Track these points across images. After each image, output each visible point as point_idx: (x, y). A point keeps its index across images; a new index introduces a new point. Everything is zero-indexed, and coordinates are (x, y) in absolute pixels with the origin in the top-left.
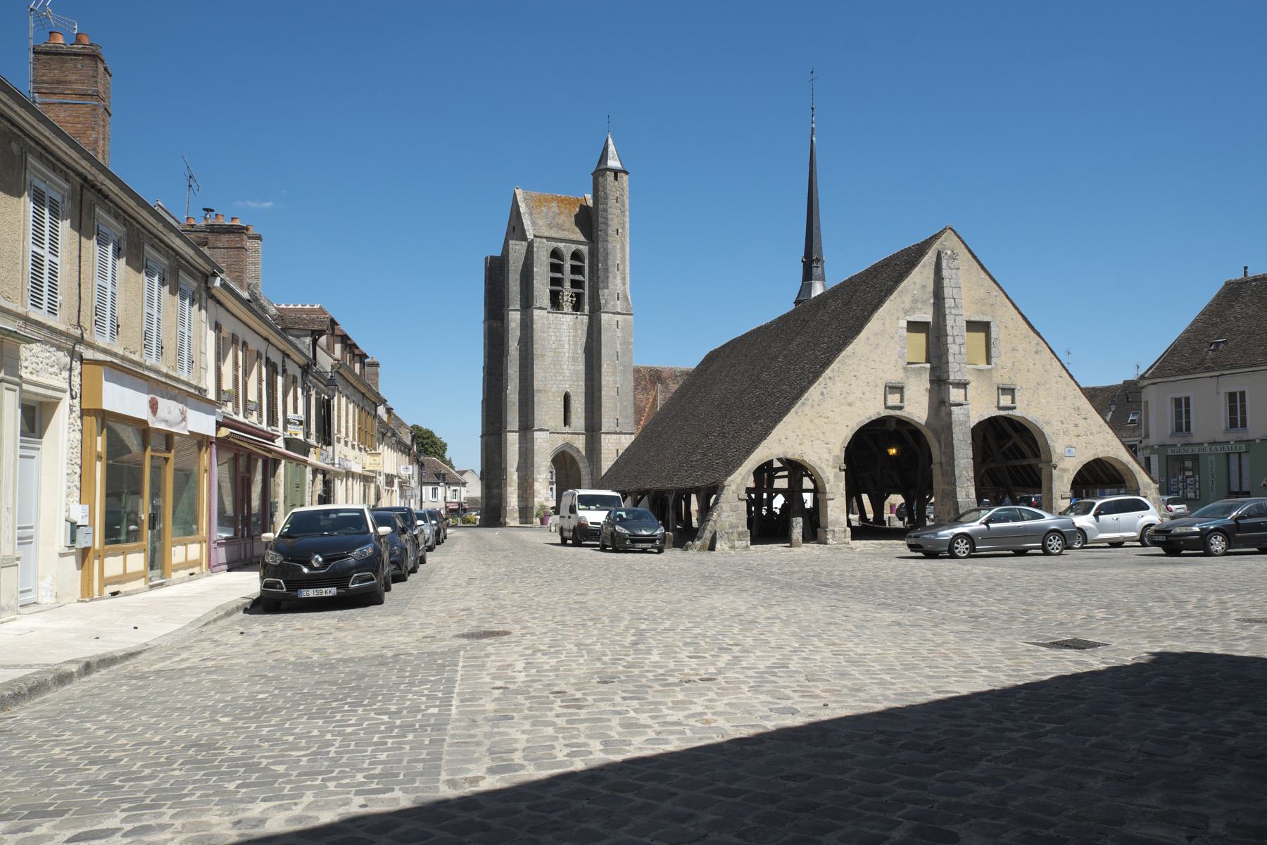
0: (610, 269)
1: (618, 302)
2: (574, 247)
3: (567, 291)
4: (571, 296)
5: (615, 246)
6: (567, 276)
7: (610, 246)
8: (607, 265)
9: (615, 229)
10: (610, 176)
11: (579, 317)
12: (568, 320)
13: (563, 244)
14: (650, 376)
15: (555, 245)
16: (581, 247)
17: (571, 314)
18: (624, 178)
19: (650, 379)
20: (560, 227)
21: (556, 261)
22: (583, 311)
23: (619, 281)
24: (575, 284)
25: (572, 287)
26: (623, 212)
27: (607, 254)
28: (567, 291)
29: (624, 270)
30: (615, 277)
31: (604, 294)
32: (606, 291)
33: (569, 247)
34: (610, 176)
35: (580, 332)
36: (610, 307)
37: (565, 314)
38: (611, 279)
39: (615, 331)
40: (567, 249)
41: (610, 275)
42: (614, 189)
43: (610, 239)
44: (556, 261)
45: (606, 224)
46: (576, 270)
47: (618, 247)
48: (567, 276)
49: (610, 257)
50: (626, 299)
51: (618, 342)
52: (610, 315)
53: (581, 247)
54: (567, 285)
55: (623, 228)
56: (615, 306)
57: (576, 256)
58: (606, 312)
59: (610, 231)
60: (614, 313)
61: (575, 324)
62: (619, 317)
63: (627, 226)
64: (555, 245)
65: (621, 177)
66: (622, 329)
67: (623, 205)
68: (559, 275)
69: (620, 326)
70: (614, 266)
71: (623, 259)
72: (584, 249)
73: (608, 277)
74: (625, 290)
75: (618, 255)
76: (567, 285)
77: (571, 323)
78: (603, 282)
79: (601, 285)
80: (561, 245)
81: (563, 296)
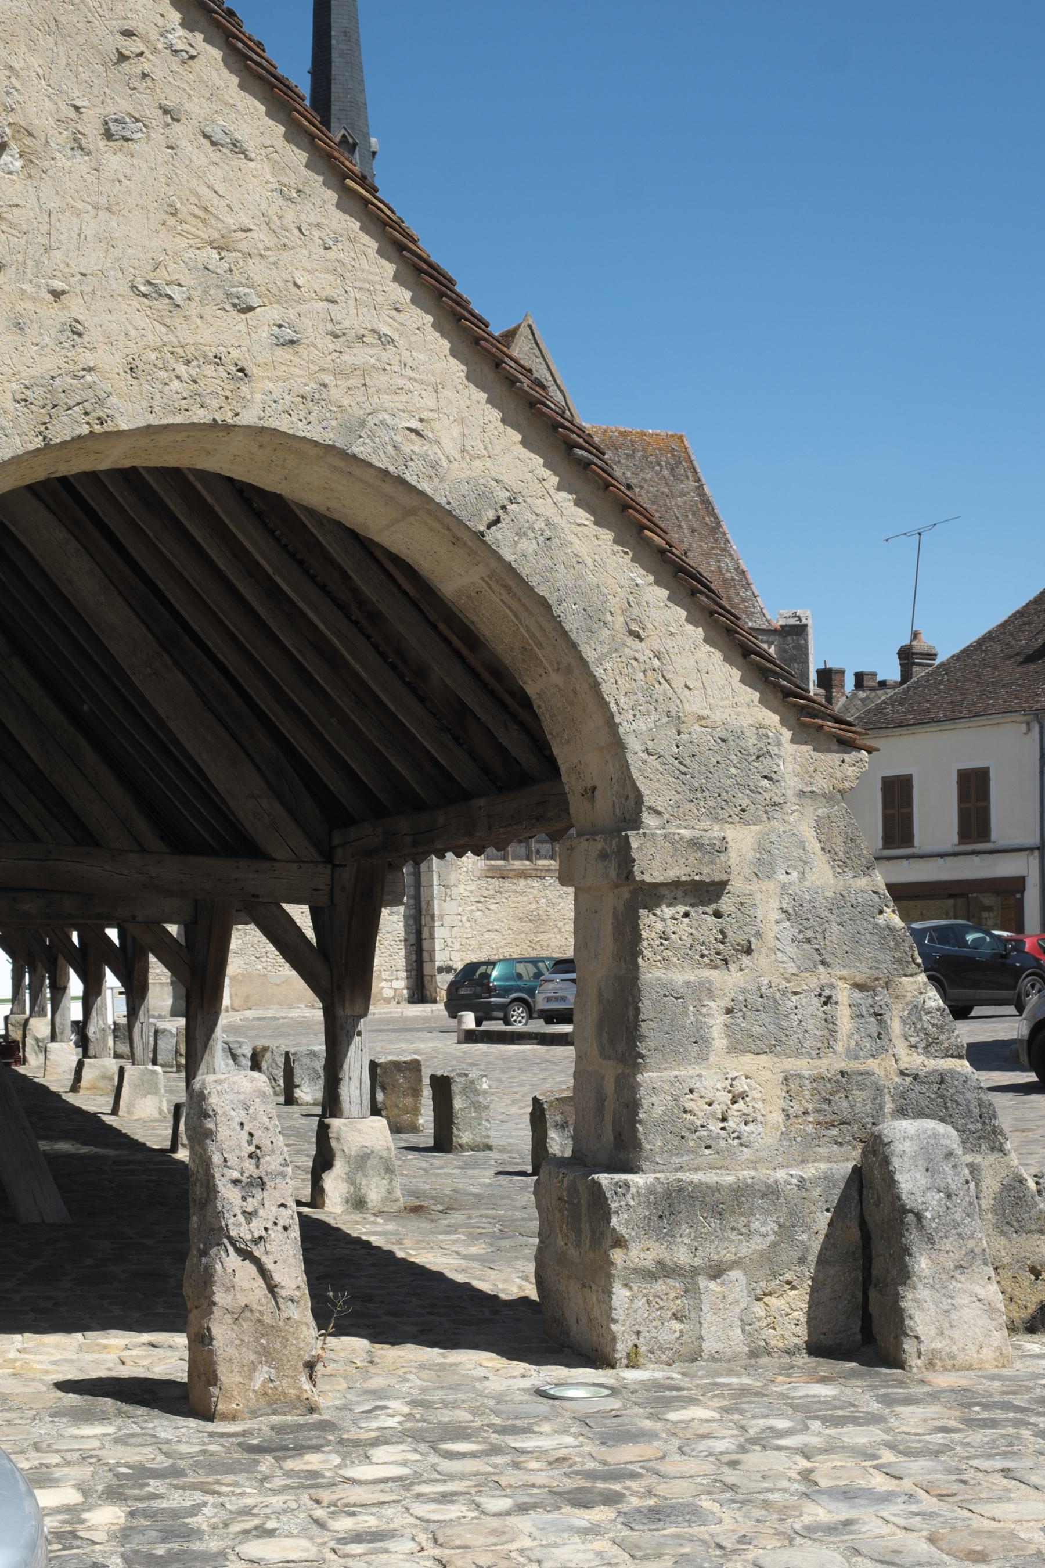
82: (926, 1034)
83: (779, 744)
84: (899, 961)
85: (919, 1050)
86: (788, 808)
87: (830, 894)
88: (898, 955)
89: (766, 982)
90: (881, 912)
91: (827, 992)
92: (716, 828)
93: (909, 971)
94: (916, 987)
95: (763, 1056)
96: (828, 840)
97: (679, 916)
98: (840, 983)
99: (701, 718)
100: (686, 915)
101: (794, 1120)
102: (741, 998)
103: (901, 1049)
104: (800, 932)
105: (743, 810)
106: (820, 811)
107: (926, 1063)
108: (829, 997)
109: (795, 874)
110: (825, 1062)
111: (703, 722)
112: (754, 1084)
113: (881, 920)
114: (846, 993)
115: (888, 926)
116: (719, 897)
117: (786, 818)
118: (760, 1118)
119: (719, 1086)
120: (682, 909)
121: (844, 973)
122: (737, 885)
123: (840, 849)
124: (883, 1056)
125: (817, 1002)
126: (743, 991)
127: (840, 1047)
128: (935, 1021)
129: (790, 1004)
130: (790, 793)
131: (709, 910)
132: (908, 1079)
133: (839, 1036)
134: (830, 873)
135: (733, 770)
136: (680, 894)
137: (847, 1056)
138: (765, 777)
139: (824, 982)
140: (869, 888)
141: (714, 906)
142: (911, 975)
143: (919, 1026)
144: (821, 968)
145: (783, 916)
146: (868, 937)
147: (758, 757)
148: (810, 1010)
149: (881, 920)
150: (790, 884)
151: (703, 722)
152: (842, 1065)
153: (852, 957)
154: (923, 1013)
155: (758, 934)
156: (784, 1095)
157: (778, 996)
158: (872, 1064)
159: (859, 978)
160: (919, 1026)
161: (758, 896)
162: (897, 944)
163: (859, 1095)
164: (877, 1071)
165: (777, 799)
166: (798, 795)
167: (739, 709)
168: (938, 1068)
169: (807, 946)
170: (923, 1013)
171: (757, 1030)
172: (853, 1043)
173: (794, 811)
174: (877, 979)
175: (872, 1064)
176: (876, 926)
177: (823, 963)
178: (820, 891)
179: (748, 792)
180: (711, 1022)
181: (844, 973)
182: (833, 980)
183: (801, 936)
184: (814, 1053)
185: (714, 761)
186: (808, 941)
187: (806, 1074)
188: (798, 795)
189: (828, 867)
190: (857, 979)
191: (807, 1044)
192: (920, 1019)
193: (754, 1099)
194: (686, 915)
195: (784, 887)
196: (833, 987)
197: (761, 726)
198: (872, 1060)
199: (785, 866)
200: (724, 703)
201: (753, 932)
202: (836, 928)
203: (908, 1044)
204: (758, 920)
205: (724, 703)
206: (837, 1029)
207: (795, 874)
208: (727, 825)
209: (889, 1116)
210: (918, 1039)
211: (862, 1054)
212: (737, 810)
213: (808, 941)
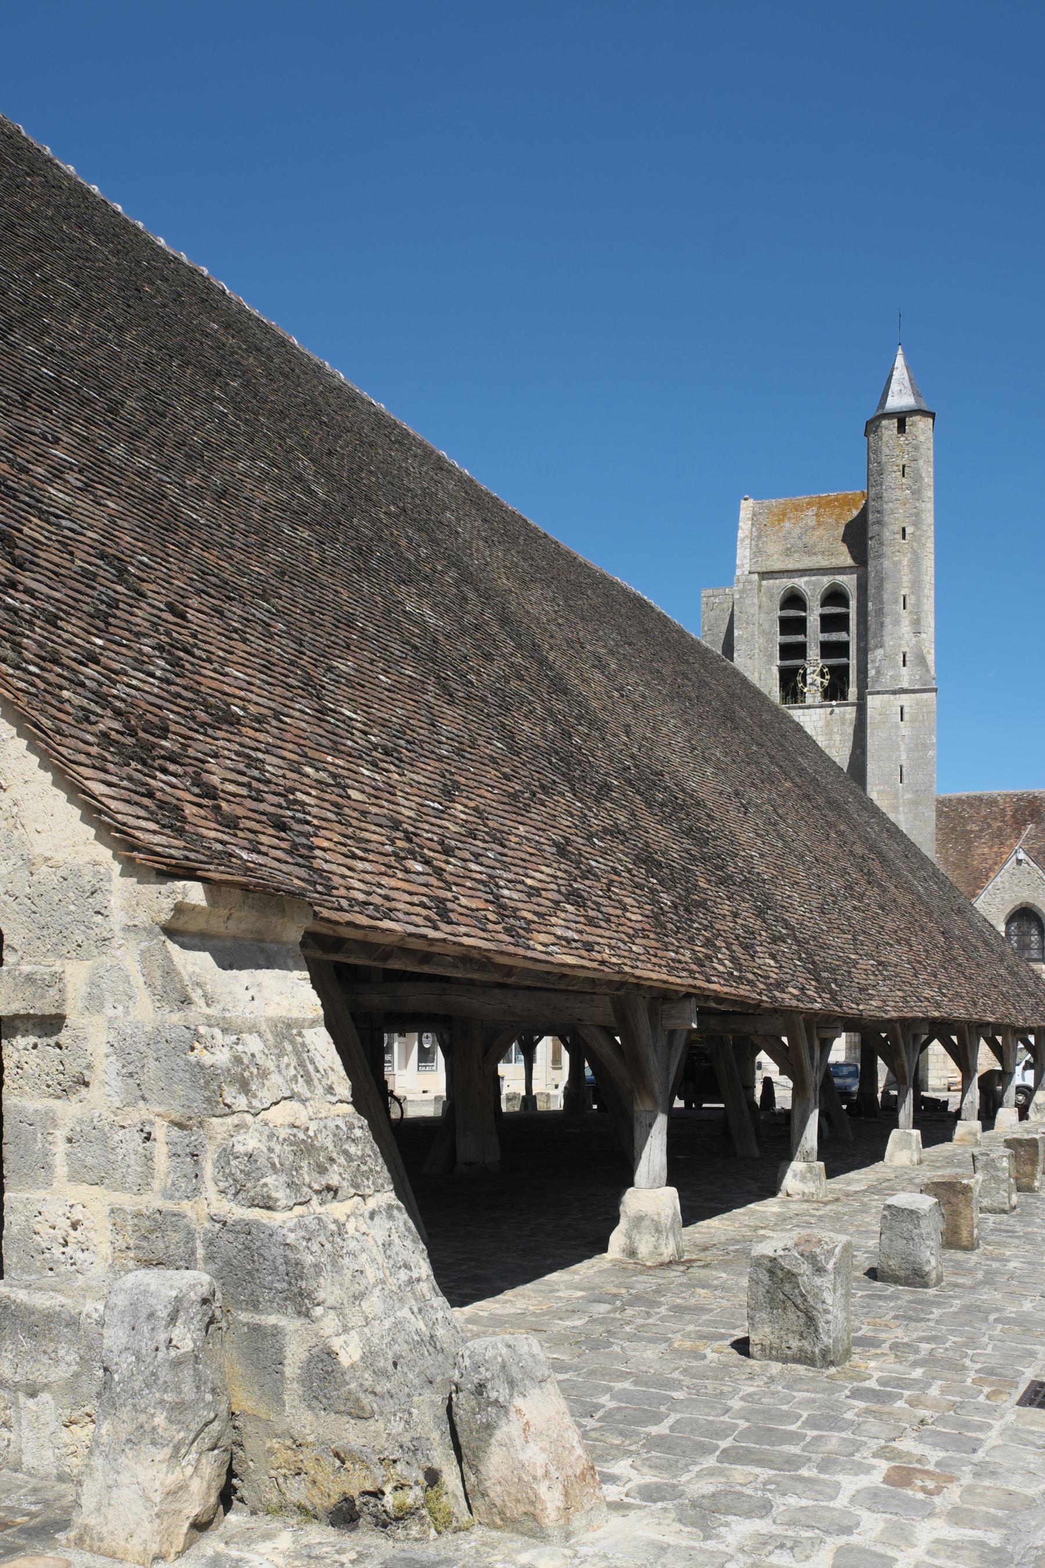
0: (887, 608)
1: (904, 671)
2: (826, 581)
3: (814, 661)
4: (822, 675)
5: (896, 564)
6: (814, 636)
7: (886, 563)
8: (881, 602)
9: (897, 528)
10: (889, 426)
11: (837, 710)
12: (814, 718)
13: (806, 579)
14: (1016, 811)
15: (788, 583)
16: (841, 579)
17: (822, 707)
18: (921, 427)
19: (1013, 816)
20: (808, 550)
21: (792, 613)
22: (844, 697)
23: (905, 628)
24: (828, 649)
25: (824, 655)
26: (917, 493)
27: (882, 580)
28: (814, 661)
29: (918, 604)
30: (897, 623)
31: (876, 656)
32: (879, 652)
33: (815, 584)
34: (889, 426)
35: (837, 737)
36: (886, 681)
37: (809, 707)
38: (888, 627)
39: (898, 727)
40: (812, 588)
41: (887, 620)
42: (897, 452)
43: (888, 550)
44: (792, 613)
45: (879, 522)
46: (830, 623)
47: (905, 562)
48: (814, 636)
49: (888, 586)
50: (921, 660)
51: (902, 747)
52: (886, 696)
53: (841, 579)
54: (813, 653)
55: (916, 524)
56: (896, 678)
57: (835, 596)
58: (878, 693)
59: (887, 534)
60: (894, 692)
61: (828, 724)
62: (905, 700)
63: (929, 518)
64: (788, 583)
65: (913, 424)
66: (912, 721)
67: (918, 478)
68: (800, 638)
69: (906, 716)
70: (896, 601)
71: (916, 584)
72: (848, 582)
73: (882, 624)
74: (918, 646)
75: (905, 579)
76: (813, 653)
77: (821, 723)
78: (875, 636)
79: (872, 643)
80: (801, 583)
81: (804, 676)
82: (235, 1180)
83: (110, 880)
84: (208, 1100)
85: (229, 1196)
86: (115, 943)
87: (148, 1029)
88: (207, 1094)
89: (97, 1114)
90: (193, 1049)
91: (147, 1129)
92: (58, 963)
93: (218, 1112)
94: (225, 1128)
95: (96, 1187)
96: (149, 974)
97: (30, 1047)
98: (157, 1119)
99: (47, 859)
100: (35, 1047)
101: (119, 1254)
102: (78, 1129)
103: (210, 1191)
104: (124, 1066)
105: (80, 946)
106: (143, 944)
107: (234, 1211)
108: (149, 1134)
109: (120, 1008)
110: (145, 1198)
111: (49, 863)
112: (88, 1214)
113: (192, 1057)
114: (164, 1130)
115: (198, 1063)
116: (60, 1030)
117: (114, 952)
118: (92, 1248)
119: (60, 1213)
120: (32, 1039)
121: (160, 1109)
122: (73, 1018)
123: (158, 983)
124: (197, 1198)
125: (139, 1138)
126: (81, 1122)
127: (156, 1185)
128: (242, 1167)
129: (117, 1138)
130: (117, 928)
131: (52, 1041)
132: (218, 1226)
133: (156, 1174)
134: (150, 1008)
135: (72, 908)
136: (30, 1026)
137: (163, 1195)
138: (98, 913)
139: (144, 1117)
140: (181, 1023)
141: (55, 1038)
142: (220, 1116)
143: (227, 1171)
144: (141, 1103)
145: (111, 1050)
146: (181, 1074)
147: (93, 893)
148: (132, 1146)
149: (192, 1057)
150: (116, 1018)
151: (49, 863)
152: (159, 1203)
153: (167, 1094)
154: (231, 1157)
155: (89, 1067)
156: (111, 1227)
157: (107, 1128)
158: (186, 1206)
159: (175, 1116)
160: (227, 1171)
161: (91, 1030)
162: (207, 1083)
163: (175, 1237)
164: (190, 1213)
165: (105, 934)
166: (123, 930)
167: (77, 848)
168: (244, 1217)
169: (130, 1081)
170: (231, 1157)
171: (90, 1161)
172: (170, 1181)
173: (121, 946)
174: (190, 1118)
175: (186, 1206)
176: (188, 1062)
177: (144, 1098)
178: (140, 1025)
179: (83, 928)
180: (55, 1150)
181: (160, 1109)
182: (152, 1117)
183: (124, 1071)
184: (135, 1189)
185: (56, 899)
186: (131, 1075)
187: (128, 1209)
188: (123, 930)
189: (149, 1001)
190: (173, 1117)
191: (130, 1179)
192: (229, 1164)
193: (86, 1228)
194: (35, 1047)
195: (110, 1021)
196: (152, 1123)
197: (96, 864)
198: (186, 1201)
199: (112, 1000)
200: (66, 843)
201: (84, 1065)
202: (152, 1064)
203: (217, 1188)
204: (88, 1053)
205: (66, 843)
206: (155, 1166)
207: (120, 1008)
208: (67, 961)
209: (200, 1262)
210: (227, 1184)
211: (177, 1195)
212: (74, 946)
213: (131, 1075)
